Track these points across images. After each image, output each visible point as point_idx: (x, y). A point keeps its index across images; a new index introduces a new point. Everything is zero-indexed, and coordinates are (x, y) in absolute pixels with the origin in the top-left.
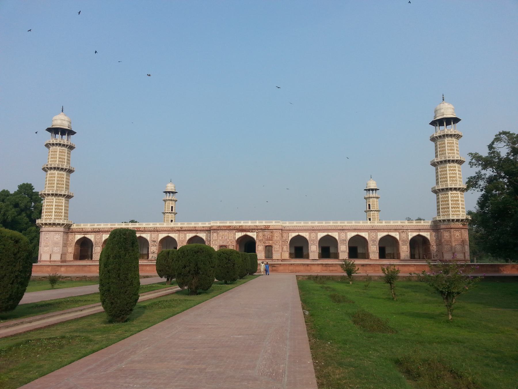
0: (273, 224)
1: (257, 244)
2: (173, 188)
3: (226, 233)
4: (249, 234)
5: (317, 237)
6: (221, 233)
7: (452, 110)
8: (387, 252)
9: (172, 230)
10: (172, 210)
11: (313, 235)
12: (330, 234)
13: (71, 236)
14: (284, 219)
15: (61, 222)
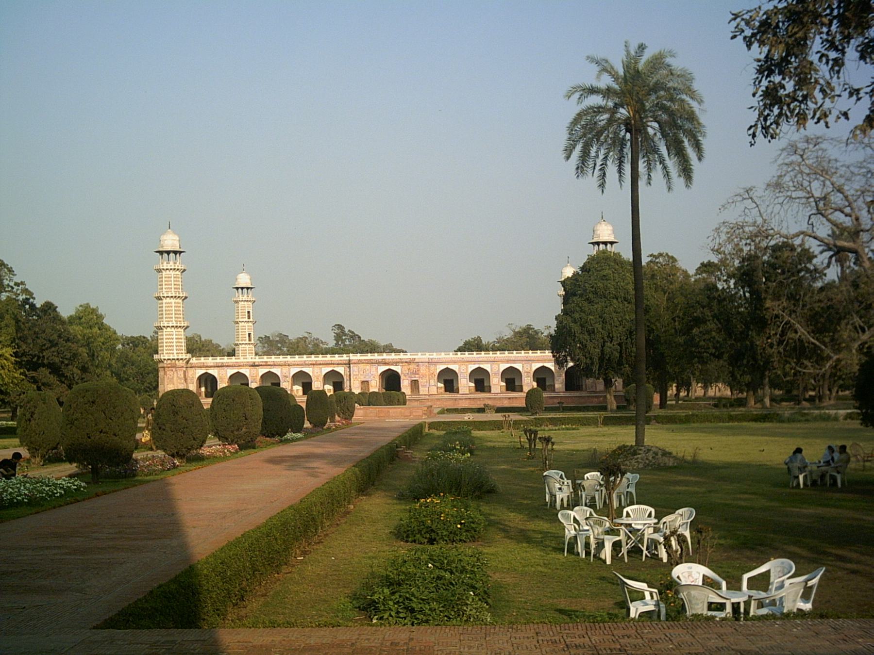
0: (419, 357)
1: (402, 377)
2: (249, 281)
3: (368, 367)
4: (393, 368)
5: (467, 369)
6: (362, 366)
7: (610, 232)
8: (547, 384)
9: (305, 364)
10: (249, 318)
11: (463, 367)
12: (482, 366)
13: (190, 372)
14: (431, 351)
15: (184, 357)
